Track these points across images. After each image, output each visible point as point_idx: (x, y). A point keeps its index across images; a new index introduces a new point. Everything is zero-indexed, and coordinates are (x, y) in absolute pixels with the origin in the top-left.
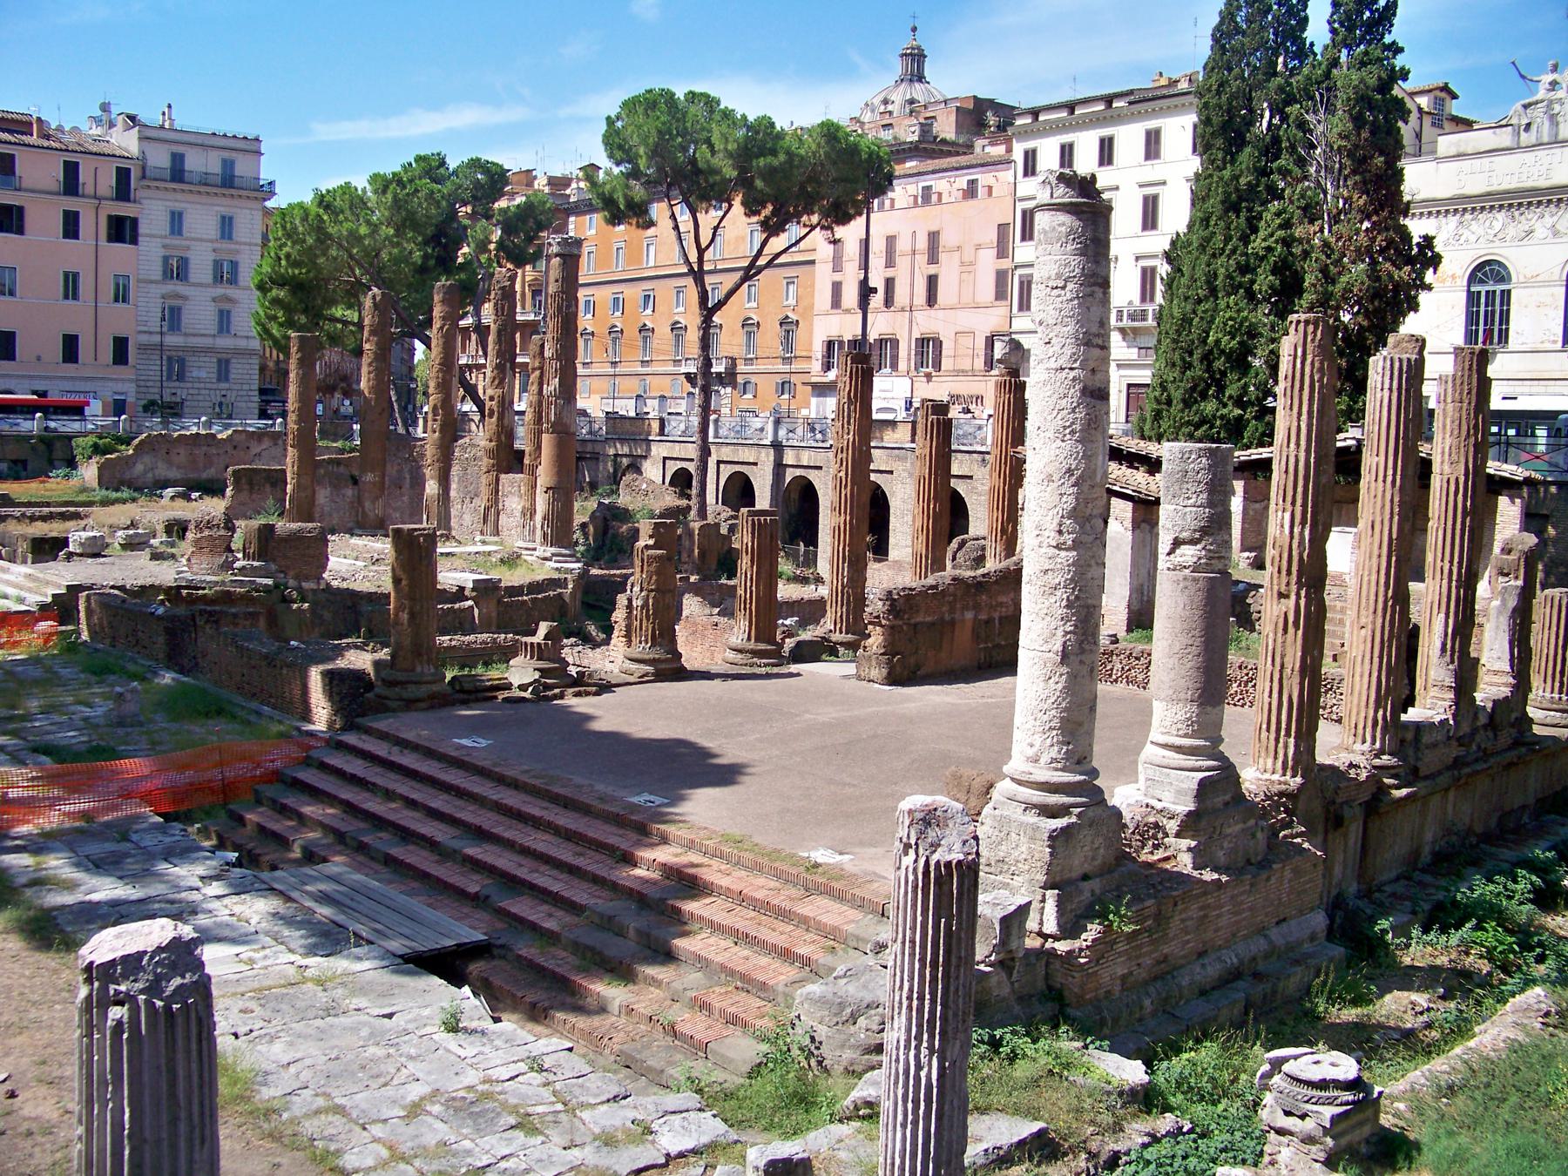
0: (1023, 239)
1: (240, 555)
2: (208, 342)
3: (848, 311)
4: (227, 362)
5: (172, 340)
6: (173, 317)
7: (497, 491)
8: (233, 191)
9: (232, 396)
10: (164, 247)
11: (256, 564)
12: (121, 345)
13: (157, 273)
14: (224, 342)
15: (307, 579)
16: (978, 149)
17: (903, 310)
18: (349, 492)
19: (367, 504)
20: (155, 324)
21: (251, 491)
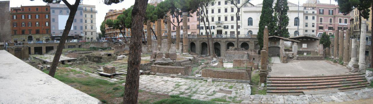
2: (90, 30)
3: (175, 23)
5: (86, 30)
9: (93, 37)
14: (92, 30)
15: (175, 60)
19: (150, 49)
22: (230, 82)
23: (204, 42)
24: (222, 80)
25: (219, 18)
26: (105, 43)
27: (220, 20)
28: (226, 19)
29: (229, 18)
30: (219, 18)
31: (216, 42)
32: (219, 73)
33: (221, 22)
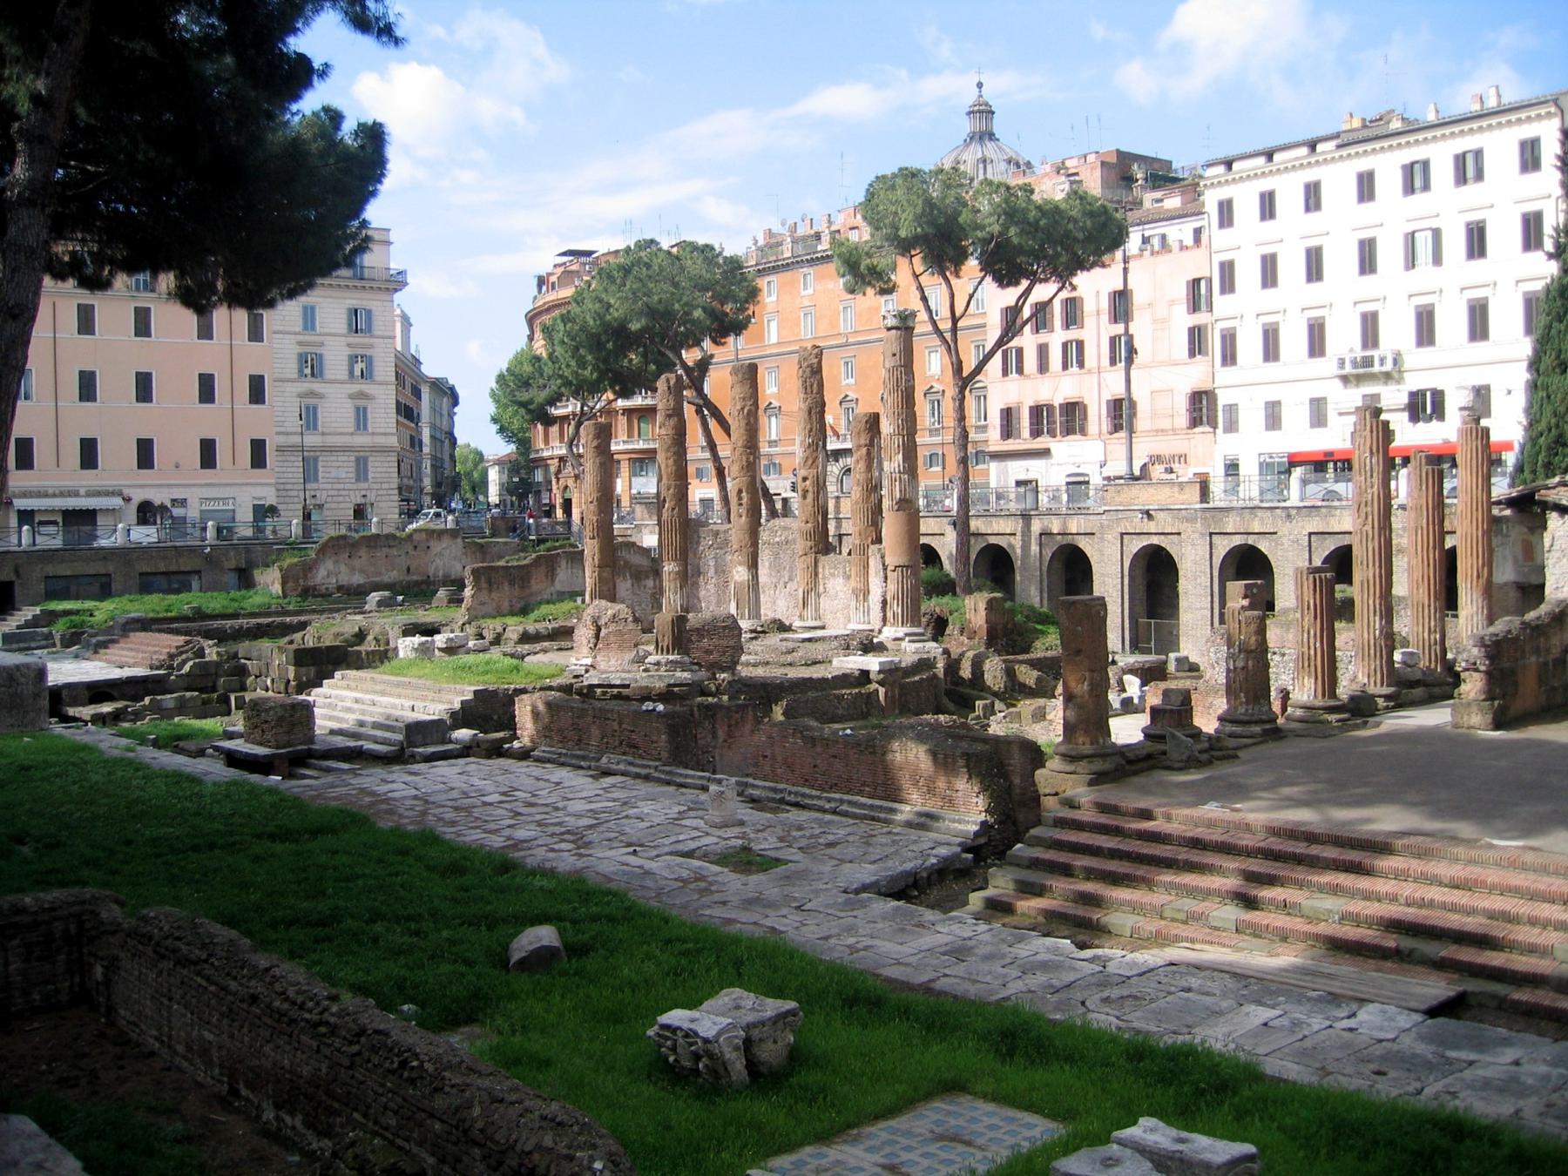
0: (1223, 291)
1: (651, 648)
3: (1028, 377)
4: (366, 459)
5: (311, 440)
6: (309, 417)
7: (816, 575)
8: (363, 283)
9: (372, 497)
10: (300, 343)
11: (671, 657)
12: (258, 447)
13: (291, 368)
14: (361, 440)
16: (1147, 204)
17: (1090, 371)
18: (650, 583)
20: (294, 424)
21: (490, 591)
22: (873, 819)
23: (1155, 540)
24: (842, 801)
25: (1370, 328)
26: (446, 541)
27: (1375, 344)
28: (1425, 329)
29: (1452, 323)
30: (1370, 328)
31: (1237, 541)
32: (832, 751)
33: (1382, 361)
